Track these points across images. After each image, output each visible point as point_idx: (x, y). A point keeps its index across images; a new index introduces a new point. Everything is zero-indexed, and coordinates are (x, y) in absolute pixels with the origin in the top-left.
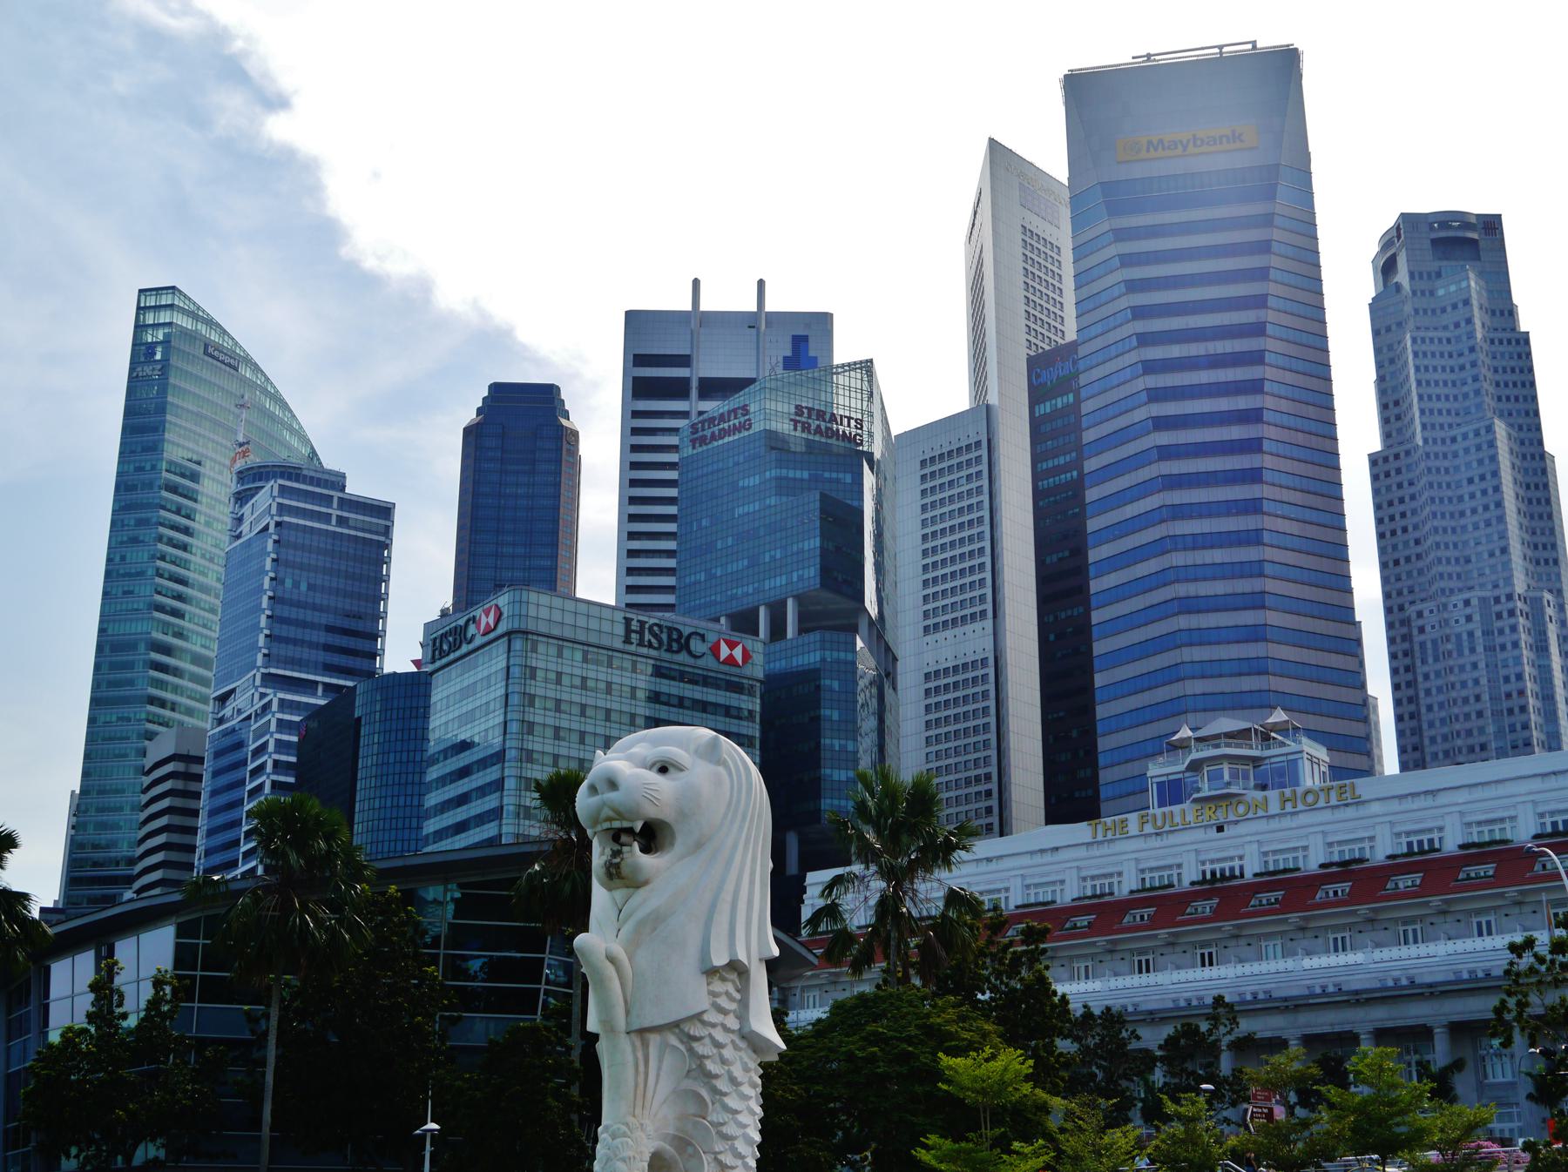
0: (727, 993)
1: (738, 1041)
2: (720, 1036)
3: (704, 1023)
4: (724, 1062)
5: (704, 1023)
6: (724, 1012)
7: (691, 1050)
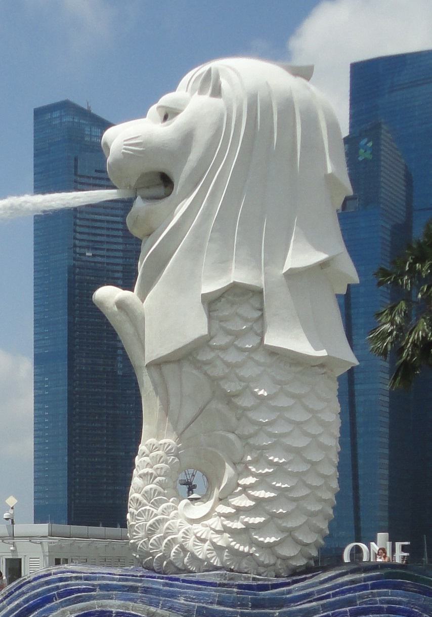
0: (237, 315)
1: (260, 357)
2: (232, 357)
3: (213, 348)
4: (241, 379)
5: (213, 348)
6: (238, 335)
7: (206, 374)
